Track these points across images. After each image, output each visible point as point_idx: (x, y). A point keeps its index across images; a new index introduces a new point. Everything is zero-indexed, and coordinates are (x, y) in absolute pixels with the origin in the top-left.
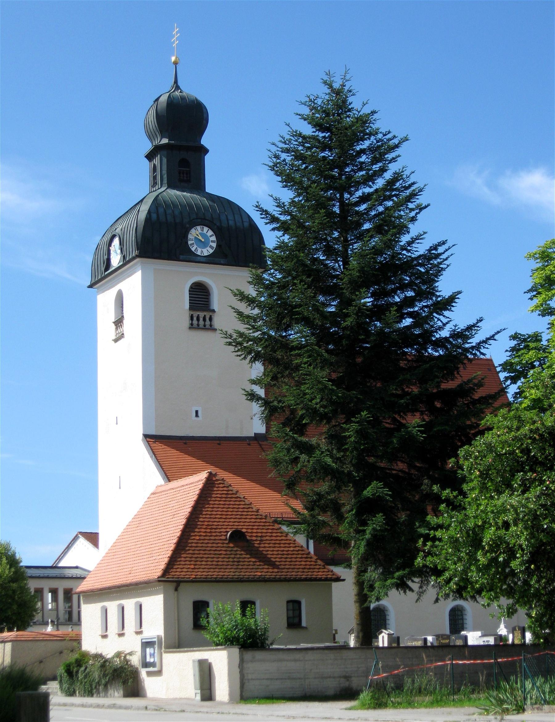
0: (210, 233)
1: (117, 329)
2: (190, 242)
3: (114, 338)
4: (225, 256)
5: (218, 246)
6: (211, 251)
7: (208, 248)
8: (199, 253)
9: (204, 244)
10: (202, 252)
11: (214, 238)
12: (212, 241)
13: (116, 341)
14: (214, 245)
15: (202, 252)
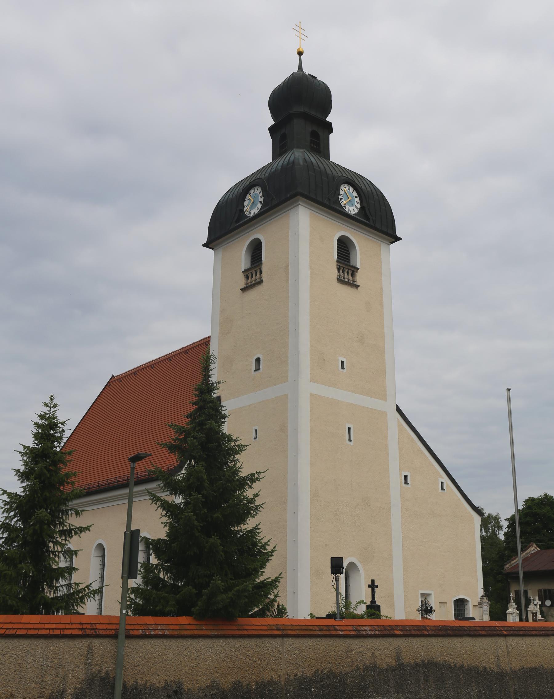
0: (355, 194)
1: (247, 277)
2: (340, 197)
3: (243, 286)
4: (368, 219)
5: (362, 208)
6: (357, 211)
7: (354, 207)
8: (347, 209)
9: (351, 203)
10: (349, 209)
11: (358, 200)
12: (357, 202)
13: (243, 290)
14: (359, 206)
15: (349, 209)
